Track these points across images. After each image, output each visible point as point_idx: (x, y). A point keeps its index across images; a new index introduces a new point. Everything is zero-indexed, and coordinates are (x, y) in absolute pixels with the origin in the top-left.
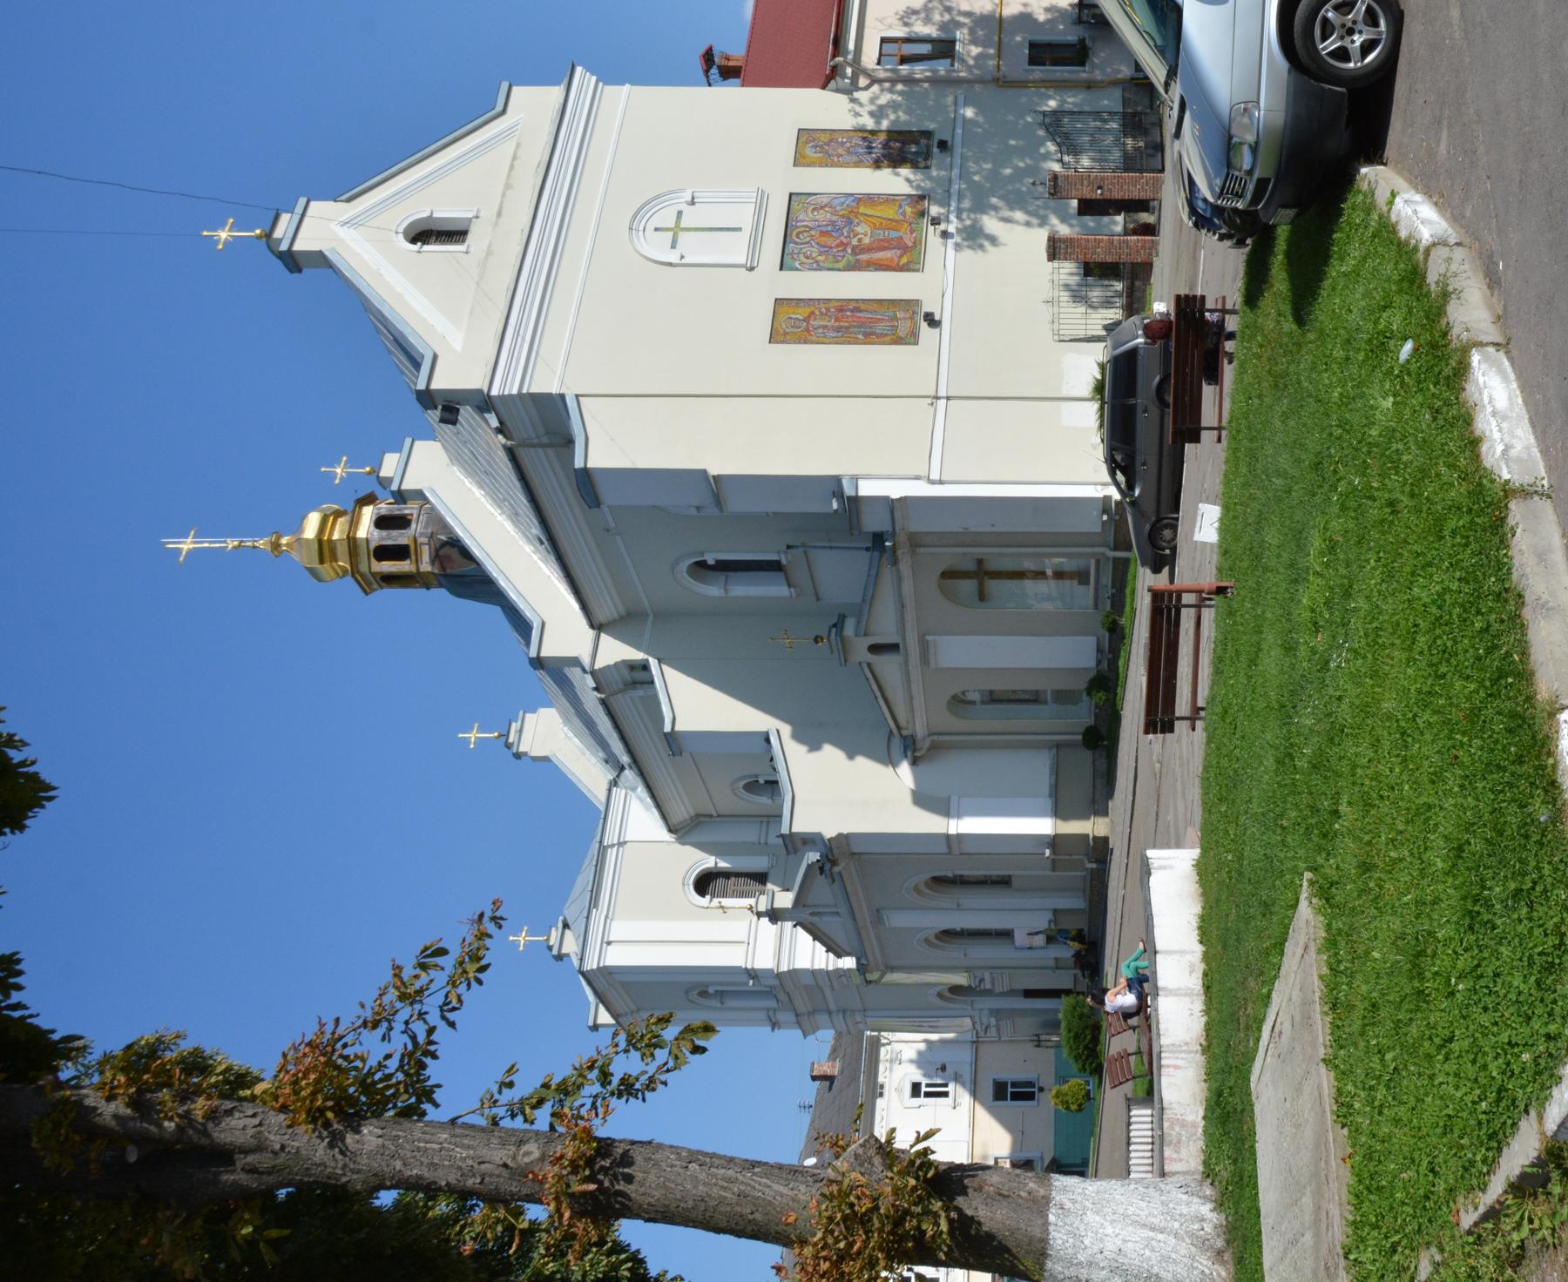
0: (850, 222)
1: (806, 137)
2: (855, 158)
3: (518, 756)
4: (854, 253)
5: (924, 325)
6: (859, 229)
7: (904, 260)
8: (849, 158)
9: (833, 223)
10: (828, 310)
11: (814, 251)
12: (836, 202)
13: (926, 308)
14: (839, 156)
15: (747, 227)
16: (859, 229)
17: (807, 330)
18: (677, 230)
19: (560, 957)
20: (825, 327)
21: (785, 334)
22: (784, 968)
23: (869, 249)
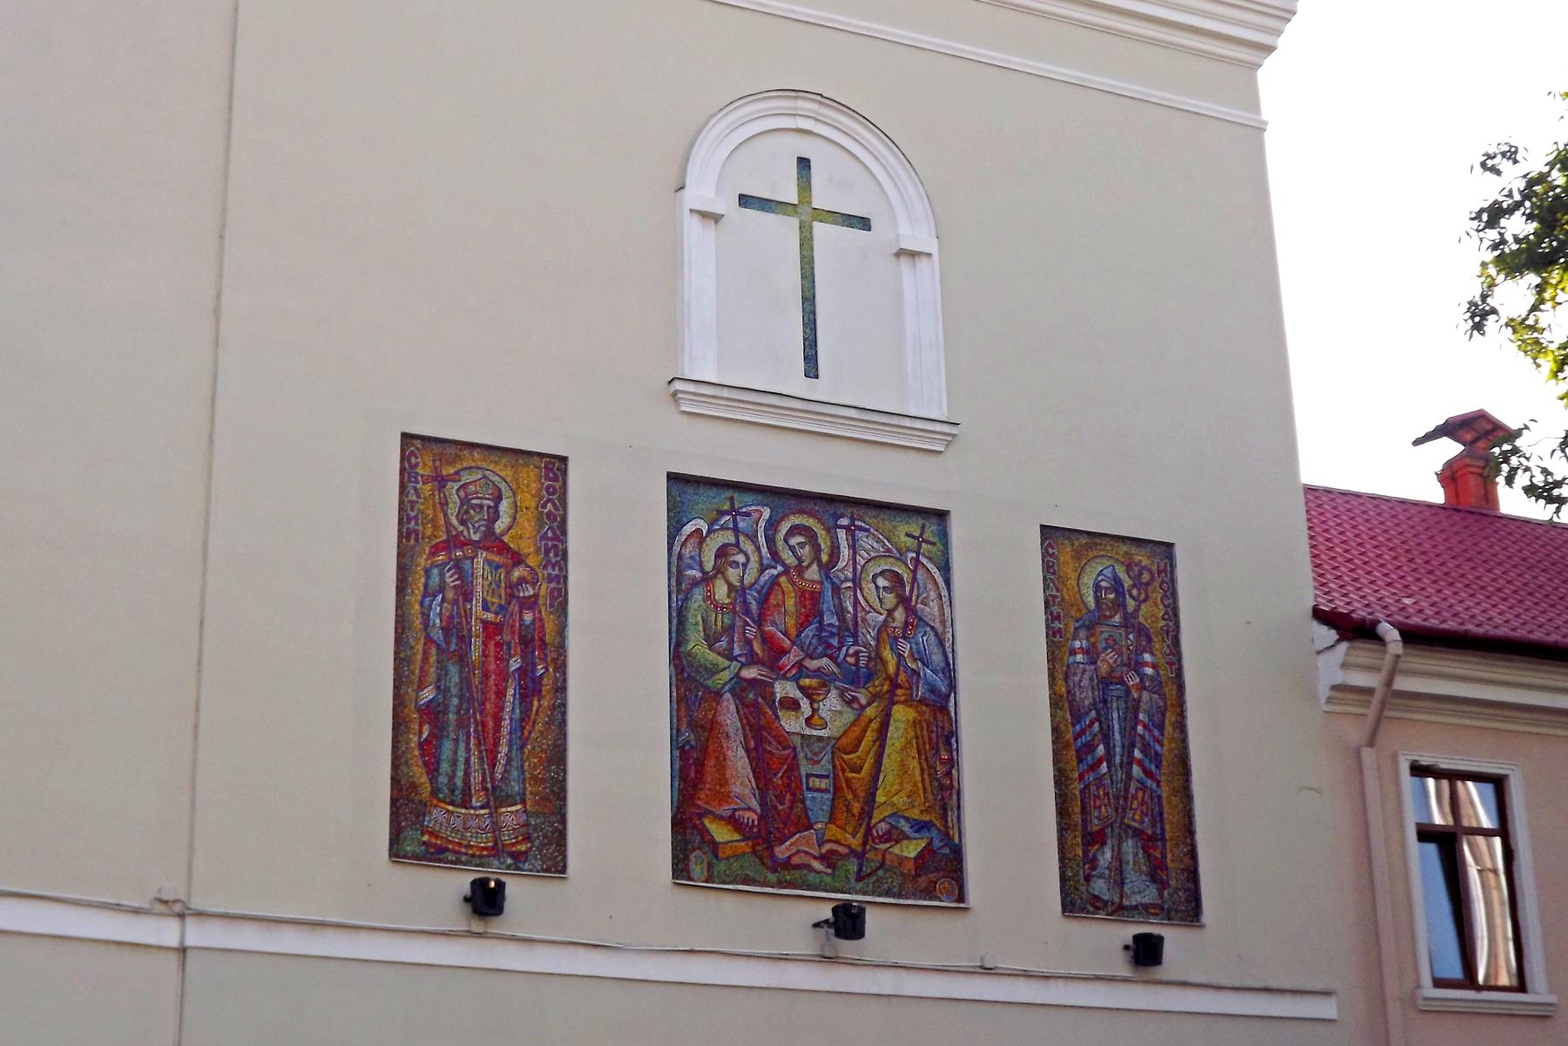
0: (855, 678)
2: (1086, 697)
4: (741, 687)
6: (831, 703)
7: (721, 833)
9: (849, 630)
10: (531, 603)
11: (748, 569)
12: (926, 640)
14: (1092, 655)
16: (831, 703)
17: (454, 542)
20: (467, 596)
21: (441, 481)
23: (760, 732)
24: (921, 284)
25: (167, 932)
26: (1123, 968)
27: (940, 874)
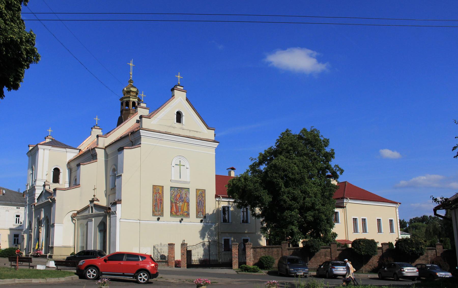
0: (183, 201)
1: (204, 191)
3: (92, 128)
4: (175, 202)
5: (157, 217)
6: (181, 203)
7: (173, 213)
8: (198, 200)
11: (175, 194)
13: (161, 218)
15: (182, 179)
16: (181, 203)
18: (180, 165)
19: (45, 138)
22: (36, 187)
23: (176, 206)
24: (188, 171)
25: (139, 221)
26: (200, 221)
27: (188, 215)
